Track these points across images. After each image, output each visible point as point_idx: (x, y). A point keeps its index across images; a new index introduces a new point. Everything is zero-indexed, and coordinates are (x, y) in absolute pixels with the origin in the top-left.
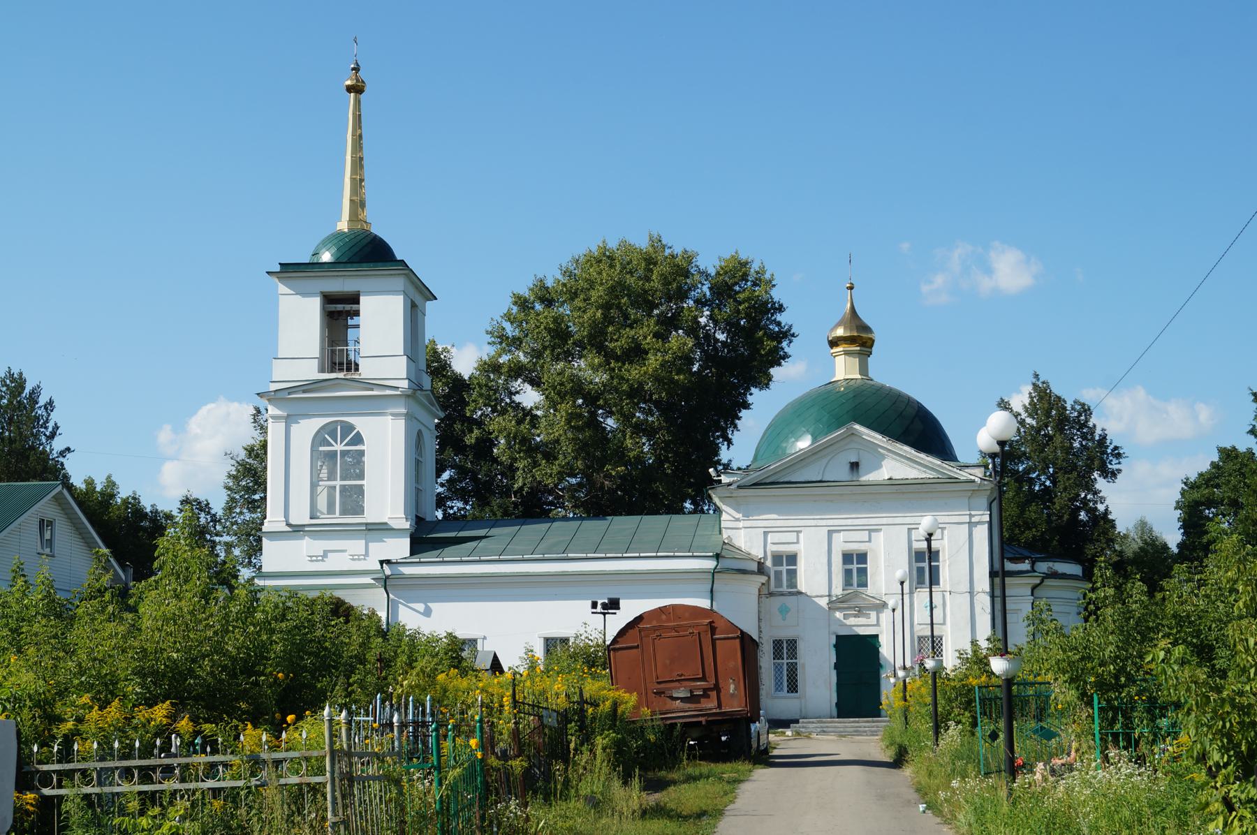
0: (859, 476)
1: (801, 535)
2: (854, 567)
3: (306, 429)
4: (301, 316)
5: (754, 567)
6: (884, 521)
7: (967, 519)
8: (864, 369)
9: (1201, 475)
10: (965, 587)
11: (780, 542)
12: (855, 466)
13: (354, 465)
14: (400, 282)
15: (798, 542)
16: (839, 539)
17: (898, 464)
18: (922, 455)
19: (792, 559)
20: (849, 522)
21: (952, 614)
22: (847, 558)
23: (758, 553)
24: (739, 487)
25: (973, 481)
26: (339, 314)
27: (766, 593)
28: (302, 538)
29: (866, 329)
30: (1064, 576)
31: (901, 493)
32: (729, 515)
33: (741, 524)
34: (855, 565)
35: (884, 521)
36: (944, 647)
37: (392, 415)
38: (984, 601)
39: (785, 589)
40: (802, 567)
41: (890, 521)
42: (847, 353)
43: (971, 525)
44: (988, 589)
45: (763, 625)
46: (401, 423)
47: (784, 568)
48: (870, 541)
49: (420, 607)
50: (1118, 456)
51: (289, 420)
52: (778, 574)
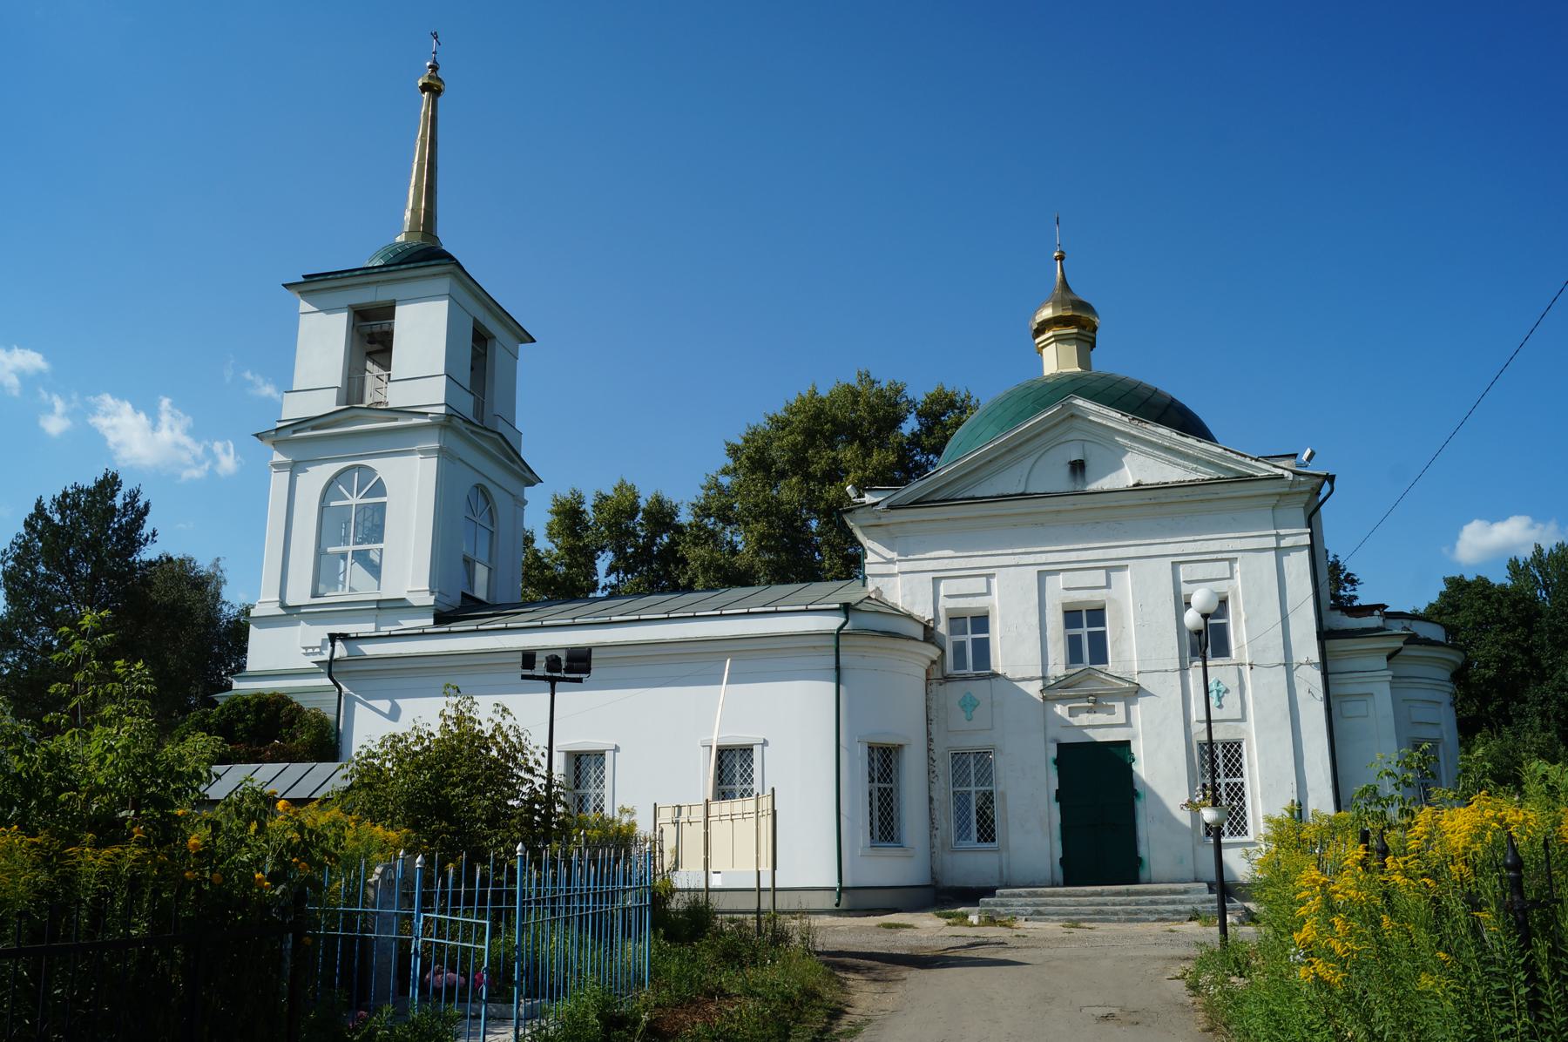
0: (1085, 483)
1: (994, 582)
2: (1084, 631)
3: (315, 478)
4: (323, 338)
5: (918, 632)
6: (1132, 552)
7: (1272, 542)
8: (1084, 361)
9: (1431, 605)
10: (1279, 657)
11: (960, 594)
12: (1078, 467)
13: (373, 524)
14: (444, 284)
15: (988, 593)
16: (1056, 584)
17: (1150, 461)
18: (1191, 441)
19: (981, 622)
20: (1073, 556)
21: (1255, 698)
22: (1072, 616)
23: (924, 611)
24: (891, 507)
25: (1282, 477)
26: (372, 338)
27: (937, 677)
28: (297, 624)
29: (1086, 307)
30: (1428, 642)
31: (1155, 507)
32: (875, 554)
33: (895, 568)
34: (1086, 629)
35: (1132, 552)
36: (1245, 760)
37: (422, 452)
38: (1310, 679)
39: (970, 670)
40: (997, 635)
41: (1142, 551)
42: (1059, 339)
43: (1280, 552)
44: (1316, 658)
45: (934, 728)
46: (432, 463)
47: (969, 638)
48: (1108, 586)
49: (385, 705)
50: (1353, 582)
51: (295, 468)
52: (959, 649)
